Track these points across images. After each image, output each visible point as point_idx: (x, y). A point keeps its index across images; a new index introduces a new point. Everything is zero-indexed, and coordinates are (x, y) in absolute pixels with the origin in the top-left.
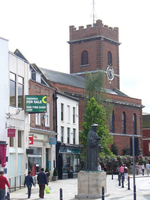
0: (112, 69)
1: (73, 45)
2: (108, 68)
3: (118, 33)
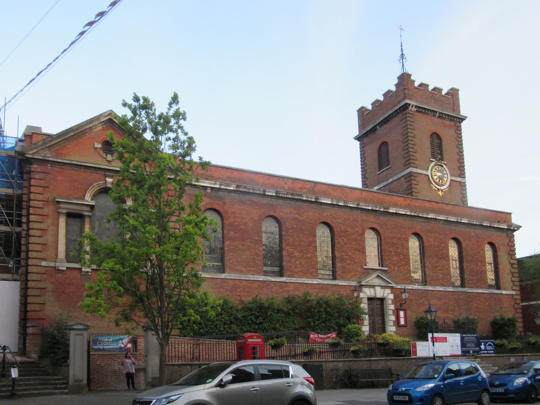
0: (444, 166)
1: (365, 140)
2: (433, 164)
3: (458, 99)
